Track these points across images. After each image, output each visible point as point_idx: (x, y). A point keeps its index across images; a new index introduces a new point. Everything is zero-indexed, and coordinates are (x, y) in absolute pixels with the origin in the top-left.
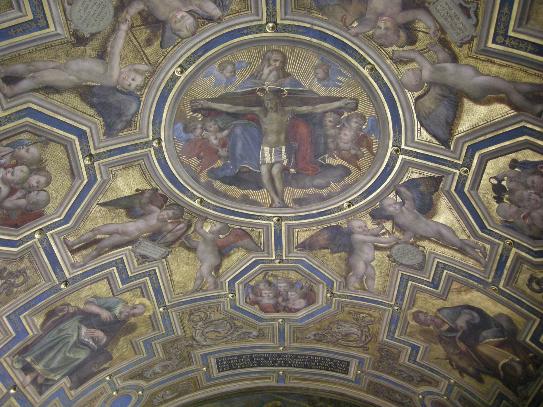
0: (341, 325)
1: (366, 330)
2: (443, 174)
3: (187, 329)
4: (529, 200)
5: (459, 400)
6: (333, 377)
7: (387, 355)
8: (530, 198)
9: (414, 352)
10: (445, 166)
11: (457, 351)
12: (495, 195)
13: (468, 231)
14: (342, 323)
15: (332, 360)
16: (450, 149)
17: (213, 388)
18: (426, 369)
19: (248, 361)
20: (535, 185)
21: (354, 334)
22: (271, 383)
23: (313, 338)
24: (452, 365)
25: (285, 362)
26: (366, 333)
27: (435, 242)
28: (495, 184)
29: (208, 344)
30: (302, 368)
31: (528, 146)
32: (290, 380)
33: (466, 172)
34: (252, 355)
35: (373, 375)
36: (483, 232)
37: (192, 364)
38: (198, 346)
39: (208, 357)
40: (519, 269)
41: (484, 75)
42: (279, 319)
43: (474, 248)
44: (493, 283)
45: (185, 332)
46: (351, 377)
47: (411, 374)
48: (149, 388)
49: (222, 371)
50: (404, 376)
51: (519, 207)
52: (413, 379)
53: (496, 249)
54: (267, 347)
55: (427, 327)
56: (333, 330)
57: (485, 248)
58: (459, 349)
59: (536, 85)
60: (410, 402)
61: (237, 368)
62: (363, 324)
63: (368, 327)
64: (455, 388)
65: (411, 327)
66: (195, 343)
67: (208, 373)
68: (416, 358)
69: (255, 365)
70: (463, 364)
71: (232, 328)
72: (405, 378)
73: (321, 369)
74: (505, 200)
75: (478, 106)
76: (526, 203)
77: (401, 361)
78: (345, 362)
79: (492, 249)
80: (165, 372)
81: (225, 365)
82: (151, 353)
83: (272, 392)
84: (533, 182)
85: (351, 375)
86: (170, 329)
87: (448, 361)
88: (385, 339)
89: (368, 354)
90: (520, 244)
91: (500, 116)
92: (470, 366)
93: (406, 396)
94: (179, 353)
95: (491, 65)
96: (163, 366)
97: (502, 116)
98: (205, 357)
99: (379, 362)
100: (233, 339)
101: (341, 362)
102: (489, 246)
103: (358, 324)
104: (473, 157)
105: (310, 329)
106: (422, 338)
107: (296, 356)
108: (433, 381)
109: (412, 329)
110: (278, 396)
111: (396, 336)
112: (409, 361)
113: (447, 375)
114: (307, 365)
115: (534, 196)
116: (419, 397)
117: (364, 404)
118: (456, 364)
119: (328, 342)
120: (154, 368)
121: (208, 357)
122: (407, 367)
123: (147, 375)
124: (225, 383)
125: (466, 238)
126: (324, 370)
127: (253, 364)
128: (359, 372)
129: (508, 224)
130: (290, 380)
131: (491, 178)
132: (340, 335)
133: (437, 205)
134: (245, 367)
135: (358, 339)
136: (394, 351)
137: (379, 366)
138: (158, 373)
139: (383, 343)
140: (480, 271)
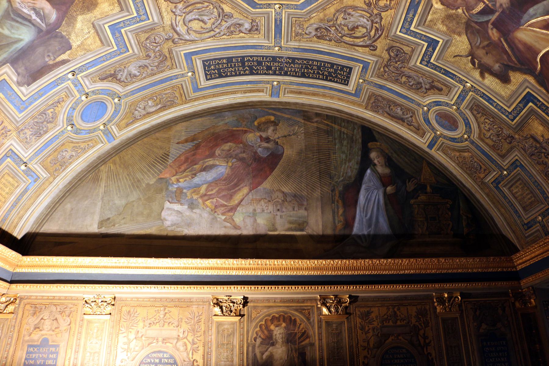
0: (349, 14)
1: (378, 20)
3: (165, 14)
5: (471, 110)
6: (331, 89)
7: (397, 55)
9: (430, 49)
11: (486, 43)
14: (350, 11)
15: (332, 65)
17: (201, 102)
18: (440, 72)
19: (238, 67)
21: (363, 27)
22: (264, 97)
23: (314, 33)
24: (473, 63)
25: (281, 69)
26: (377, 25)
29: (191, 39)
30: (298, 77)
32: (284, 94)
34: (243, 57)
35: (376, 85)
37: (174, 66)
38: (180, 41)
39: (193, 57)
42: (275, 4)
45: (162, 18)
46: (351, 89)
47: (421, 80)
48: (126, 96)
49: (210, 79)
50: (411, 84)
52: (422, 87)
54: (261, 47)
55: (454, 11)
56: (339, 22)
58: (489, 38)
60: (411, 117)
61: (227, 76)
62: (375, 12)
63: (380, 15)
64: (471, 93)
65: (434, 13)
66: (176, 36)
67: (194, 81)
68: (430, 58)
69: (247, 72)
70: (488, 60)
71: (219, 17)
72: (412, 86)
73: (319, 79)
77: (412, 63)
78: (347, 67)
80: (144, 75)
81: (214, 70)
82: (123, 46)
83: (266, 107)
85: (351, 87)
86: (142, 12)
87: (470, 58)
88: (398, 33)
89: (374, 55)
92: (497, 62)
93: (409, 110)
94: (157, 49)
96: (140, 67)
98: (189, 56)
99: (386, 66)
100: (222, 33)
101: (343, 67)
103: (370, 11)
105: (312, 21)
106: (444, 29)
107: (293, 60)
108: (444, 88)
109: (435, 16)
110: (271, 111)
111: (412, 28)
112: (421, 63)
113: (464, 78)
114: (304, 72)
116: (423, 109)
117: (361, 121)
118: (480, 62)
119: (330, 40)
120: (129, 68)
121: (193, 57)
122: (417, 71)
123: (123, 76)
124: (214, 96)
126: (323, 79)
127: (245, 71)
128: (361, 81)
130: (284, 94)
132: (346, 28)
134: (236, 75)
135: (366, 35)
136: (405, 49)
137: (385, 72)
138: (135, 76)
139: (397, 39)
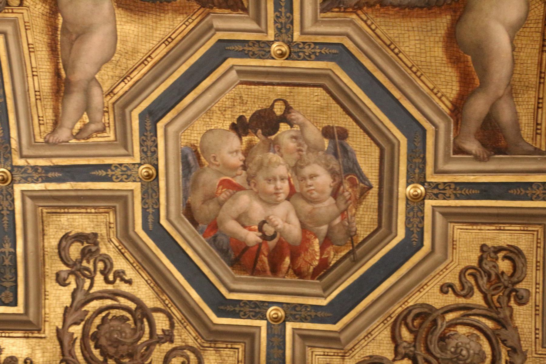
2: (251, 10)
4: (272, 179)
8: (275, 179)
10: (276, 10)
12: (248, 118)
13: (126, 88)
16: (323, 11)
20: (309, 182)
27: (53, 29)
28: (274, 113)
31: (387, 149)
33: (282, 55)
36: (142, 116)
40: (95, 207)
41: (512, 40)
43: (87, 108)
44: (13, 168)
51: (244, 167)
53: (112, 152)
57: (103, 130)
59: (519, 130)
74: (245, 139)
75: (441, 45)
76: (261, 178)
79: (109, 144)
84: (312, 176)
90: (157, 192)
91: (431, 86)
95: (537, 47)
97: (432, 90)
102: (112, 138)
104: (318, 59)
115: (284, 186)
125: (105, 89)
129: (190, 158)
131: (285, 102)
133: (165, 11)
140: (31, 135)
